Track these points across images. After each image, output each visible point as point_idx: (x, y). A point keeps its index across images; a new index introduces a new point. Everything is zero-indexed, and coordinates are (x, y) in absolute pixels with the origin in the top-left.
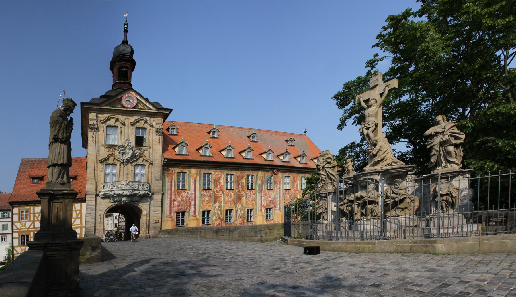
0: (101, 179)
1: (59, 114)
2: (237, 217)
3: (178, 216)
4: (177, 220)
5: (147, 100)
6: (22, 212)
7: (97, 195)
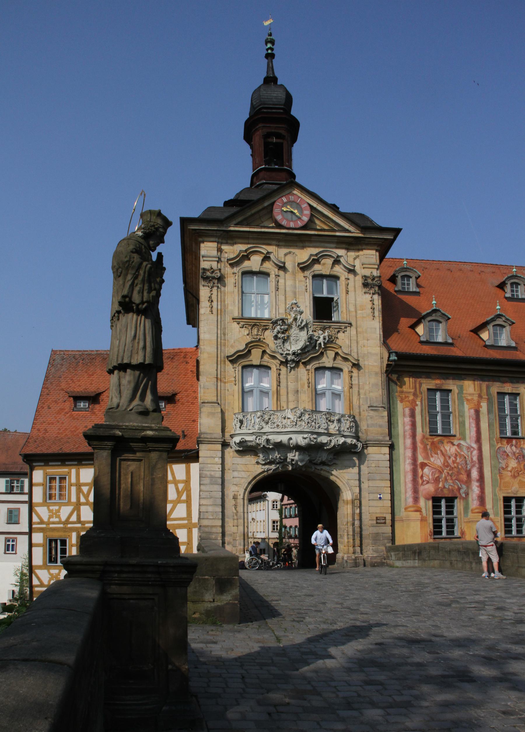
0: (233, 403)
1: (131, 247)
3: (436, 510)
4: (435, 521)
5: (334, 208)
6: (52, 479)
7: (225, 445)
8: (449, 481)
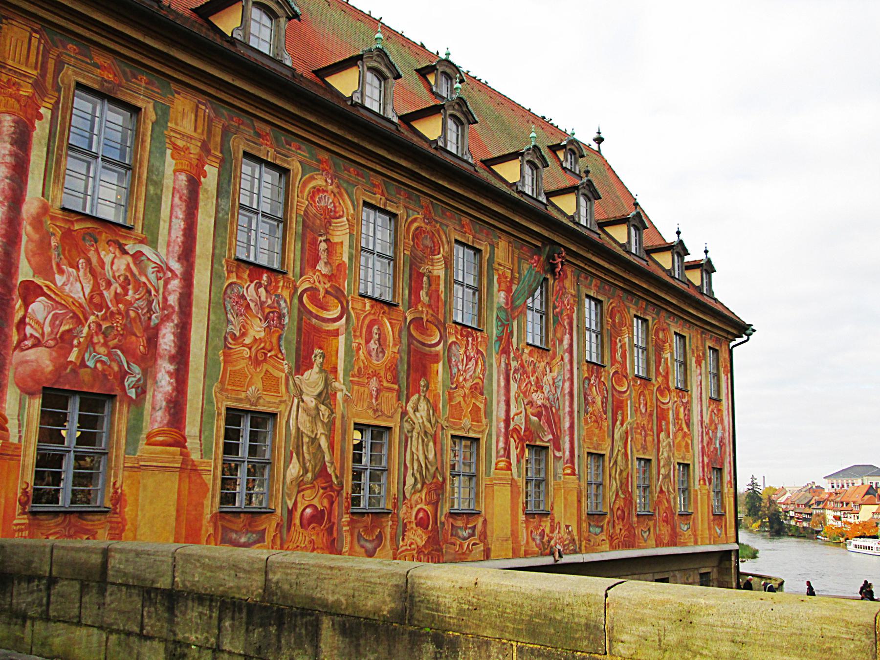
2: (410, 481)
8: (97, 348)
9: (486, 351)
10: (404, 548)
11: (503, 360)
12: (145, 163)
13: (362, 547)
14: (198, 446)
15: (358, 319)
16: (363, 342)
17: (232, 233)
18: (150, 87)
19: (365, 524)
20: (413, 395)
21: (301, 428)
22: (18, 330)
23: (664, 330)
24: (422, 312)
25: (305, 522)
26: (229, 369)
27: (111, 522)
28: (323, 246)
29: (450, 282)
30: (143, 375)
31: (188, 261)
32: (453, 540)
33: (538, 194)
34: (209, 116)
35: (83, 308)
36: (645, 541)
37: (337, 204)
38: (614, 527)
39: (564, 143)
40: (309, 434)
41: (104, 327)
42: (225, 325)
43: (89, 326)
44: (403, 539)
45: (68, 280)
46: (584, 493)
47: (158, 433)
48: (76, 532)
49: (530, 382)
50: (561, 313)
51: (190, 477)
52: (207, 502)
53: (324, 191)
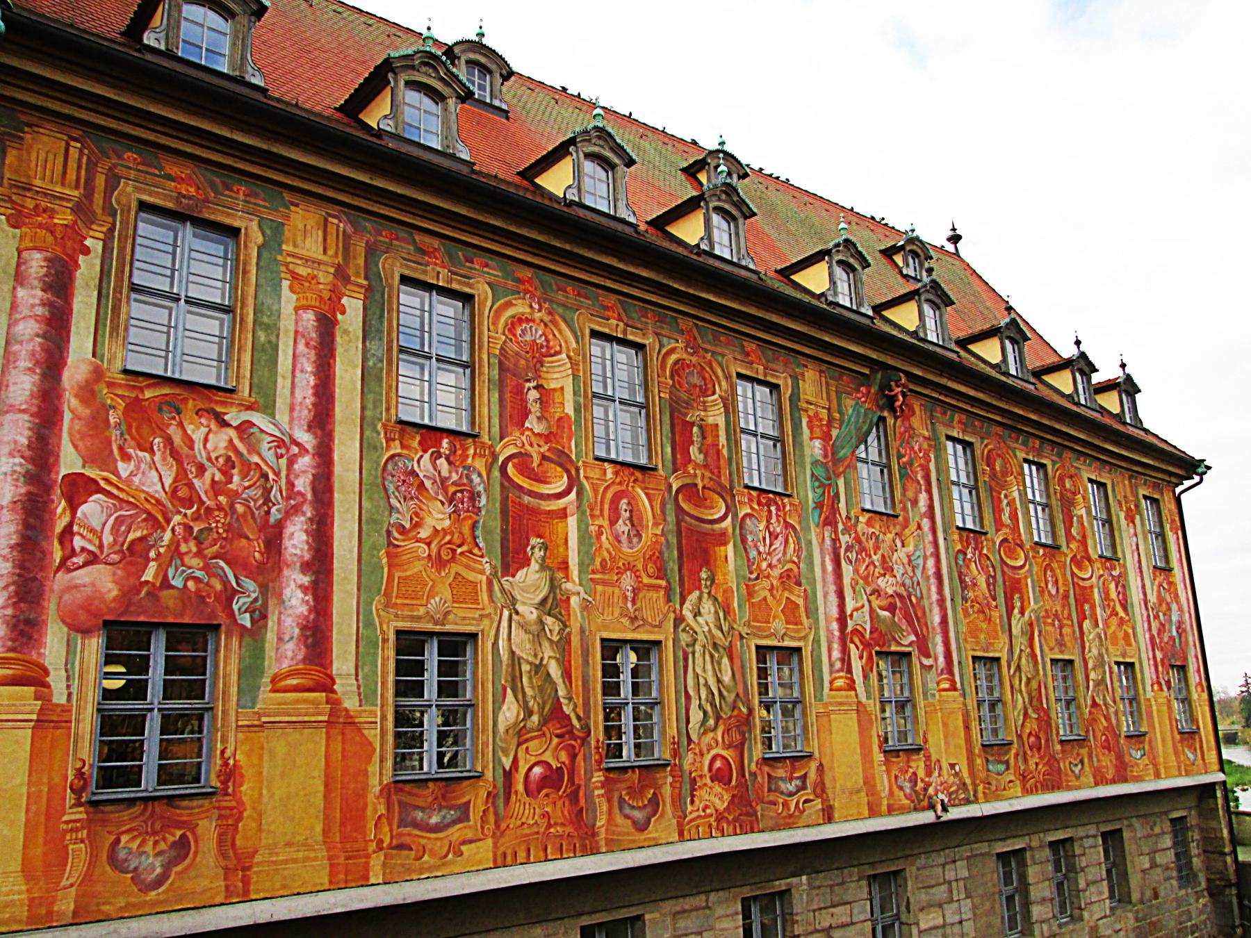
2: (696, 716)
9: (800, 523)
10: (695, 815)
11: (827, 534)
12: (251, 301)
13: (627, 817)
14: (355, 688)
15: (596, 492)
16: (606, 523)
17: (390, 387)
18: (253, 200)
19: (628, 784)
20: (690, 592)
21: (518, 652)
22: (61, 543)
23: (1071, 477)
24: (695, 475)
25: (533, 786)
26: (397, 575)
27: (219, 808)
28: (533, 395)
29: (734, 432)
30: (261, 592)
31: (322, 428)
32: (771, 798)
33: (860, 304)
34: (344, 231)
35: (163, 505)
36: (1078, 778)
37: (551, 337)
38: (1026, 761)
39: (902, 243)
40: (531, 659)
41: (196, 530)
42: (387, 513)
43: (173, 530)
44: (692, 802)
45: (138, 468)
46: (974, 714)
47: (290, 674)
48: (164, 827)
49: (873, 563)
50: (910, 464)
51: (343, 734)
52: (374, 768)
53: (528, 320)
